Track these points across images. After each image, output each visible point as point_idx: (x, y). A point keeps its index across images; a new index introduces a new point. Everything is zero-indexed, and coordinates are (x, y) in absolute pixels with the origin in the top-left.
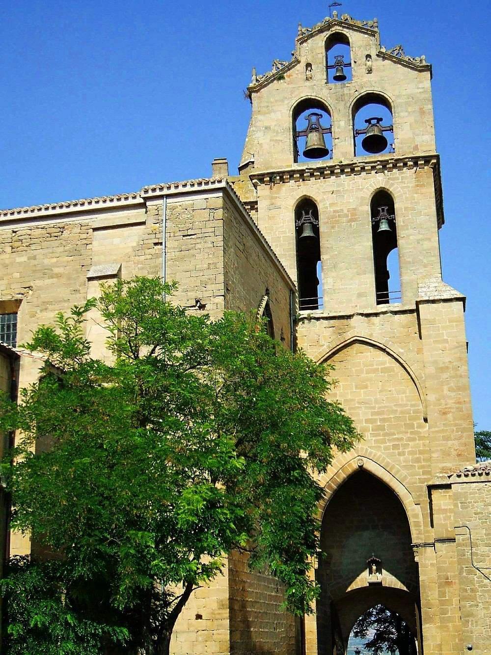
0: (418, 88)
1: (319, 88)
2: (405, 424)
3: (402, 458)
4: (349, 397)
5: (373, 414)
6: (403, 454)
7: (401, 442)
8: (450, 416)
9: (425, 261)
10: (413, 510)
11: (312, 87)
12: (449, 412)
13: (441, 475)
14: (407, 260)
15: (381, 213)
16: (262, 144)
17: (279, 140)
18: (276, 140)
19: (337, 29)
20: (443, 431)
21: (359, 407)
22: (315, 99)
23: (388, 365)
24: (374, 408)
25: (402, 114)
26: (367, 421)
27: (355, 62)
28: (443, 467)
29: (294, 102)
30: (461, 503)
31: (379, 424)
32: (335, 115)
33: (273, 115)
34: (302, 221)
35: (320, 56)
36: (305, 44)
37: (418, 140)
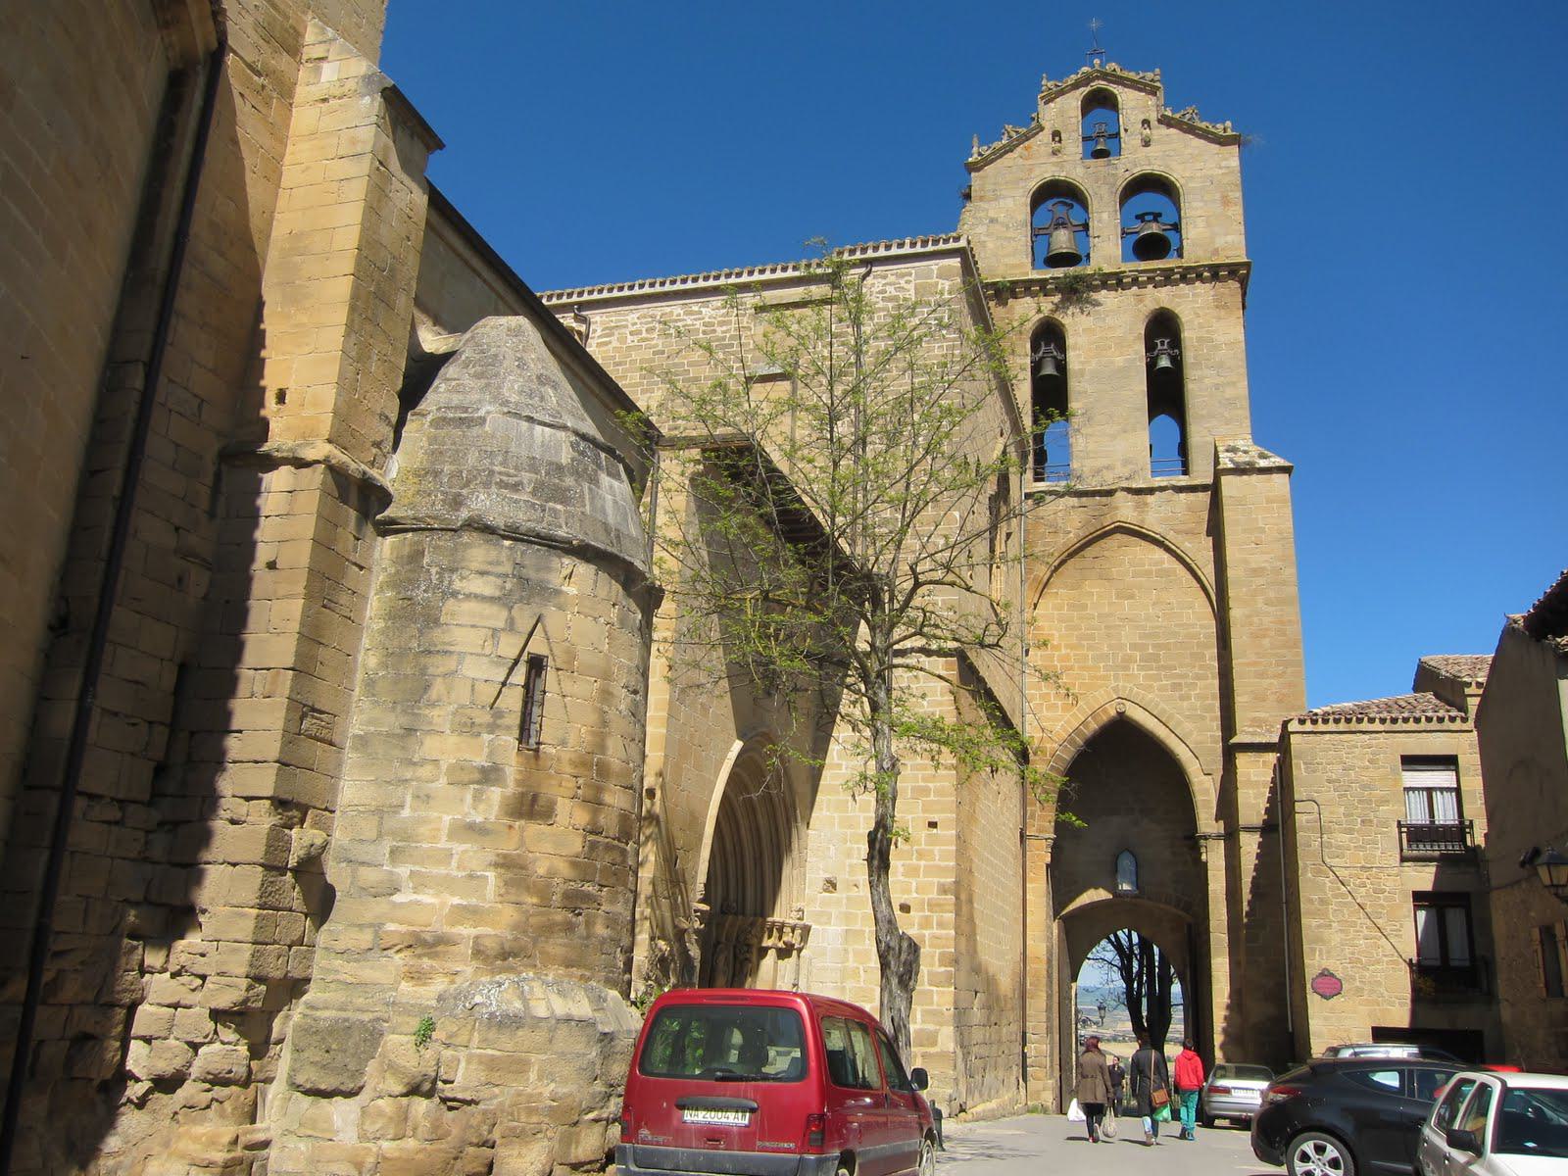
0: (1220, 168)
1: (1073, 167)
3: (1185, 704)
4: (1107, 610)
8: (1266, 642)
9: (1226, 415)
10: (1201, 783)
11: (1060, 165)
12: (1264, 636)
13: (1251, 729)
14: (1200, 413)
15: (1159, 347)
16: (985, 242)
17: (1010, 238)
18: (1006, 238)
19: (1101, 84)
20: (1254, 664)
21: (1119, 626)
22: (1064, 181)
23: (1166, 565)
25: (1194, 204)
26: (1134, 647)
27: (1126, 130)
29: (1033, 184)
30: (1305, 763)
32: (1094, 205)
34: (1041, 354)
35: (1074, 120)
36: (1052, 105)
37: (1220, 242)
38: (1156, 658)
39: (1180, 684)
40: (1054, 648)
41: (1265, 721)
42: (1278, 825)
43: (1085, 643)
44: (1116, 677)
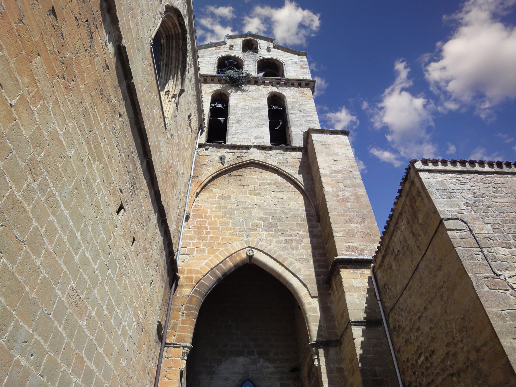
2: (296, 224)
3: (295, 252)
5: (264, 214)
6: (297, 248)
7: (294, 238)
10: (310, 304)
12: (348, 202)
21: (251, 208)
23: (280, 181)
24: (267, 209)
26: (260, 219)
27: (260, 48)
28: (349, 246)
31: (271, 221)
33: (205, 58)
38: (274, 225)
39: (291, 240)
40: (206, 217)
41: (357, 248)
42: (382, 319)
43: (228, 216)
44: (248, 235)
